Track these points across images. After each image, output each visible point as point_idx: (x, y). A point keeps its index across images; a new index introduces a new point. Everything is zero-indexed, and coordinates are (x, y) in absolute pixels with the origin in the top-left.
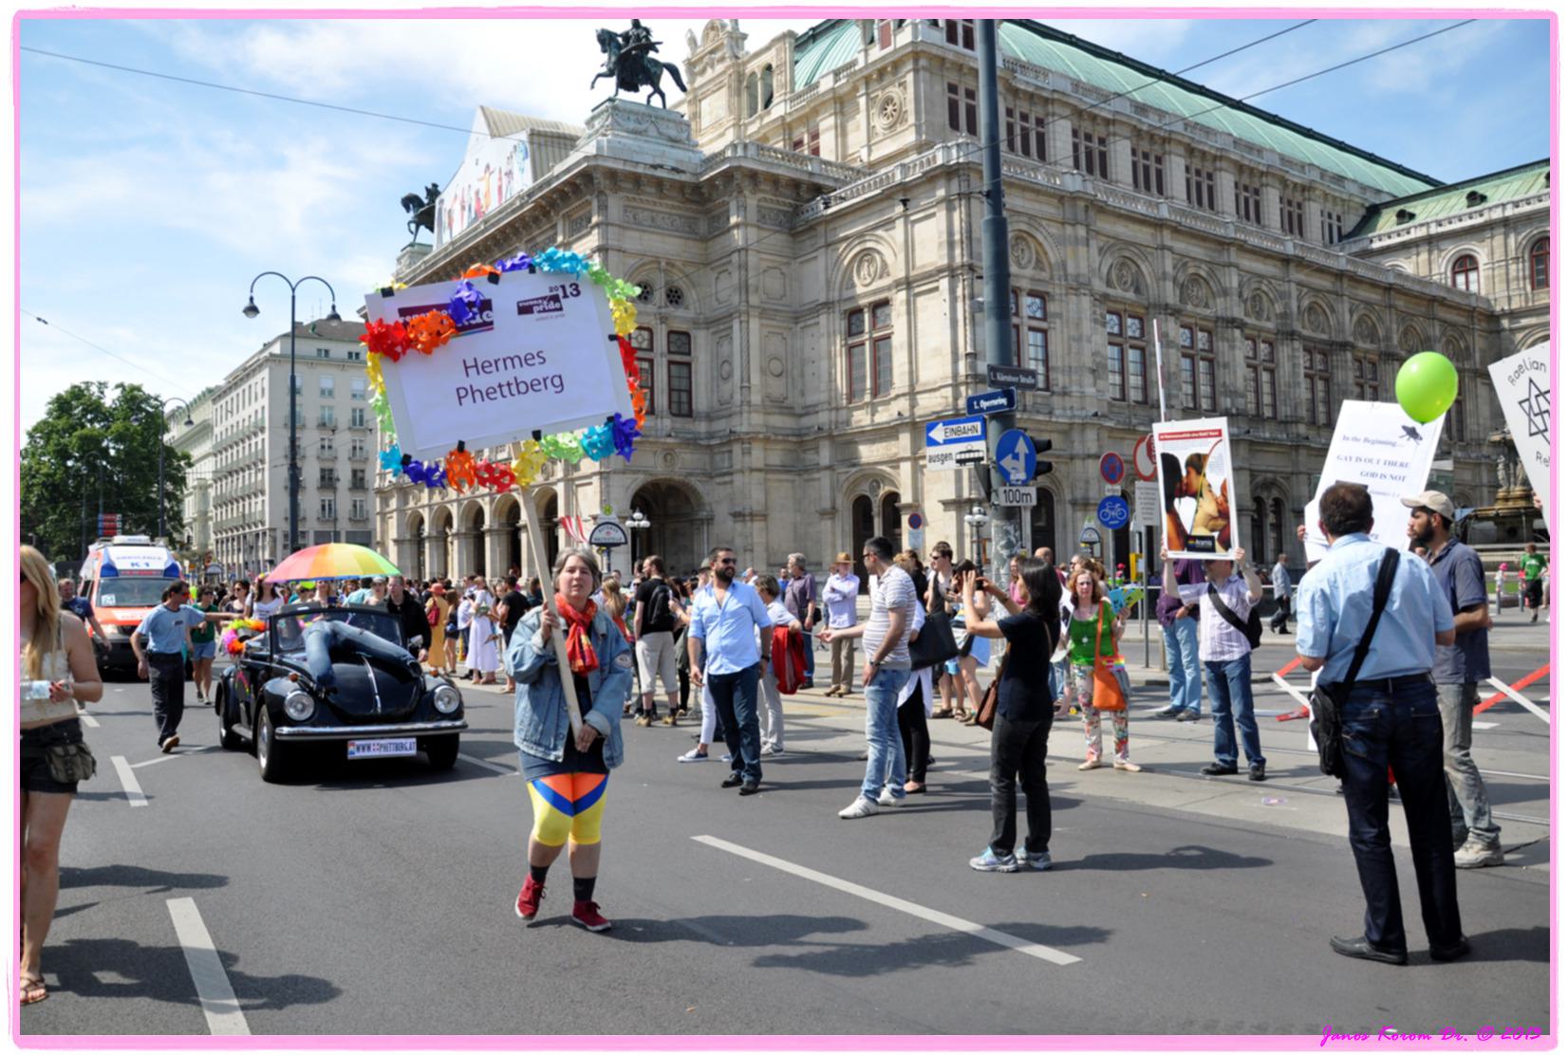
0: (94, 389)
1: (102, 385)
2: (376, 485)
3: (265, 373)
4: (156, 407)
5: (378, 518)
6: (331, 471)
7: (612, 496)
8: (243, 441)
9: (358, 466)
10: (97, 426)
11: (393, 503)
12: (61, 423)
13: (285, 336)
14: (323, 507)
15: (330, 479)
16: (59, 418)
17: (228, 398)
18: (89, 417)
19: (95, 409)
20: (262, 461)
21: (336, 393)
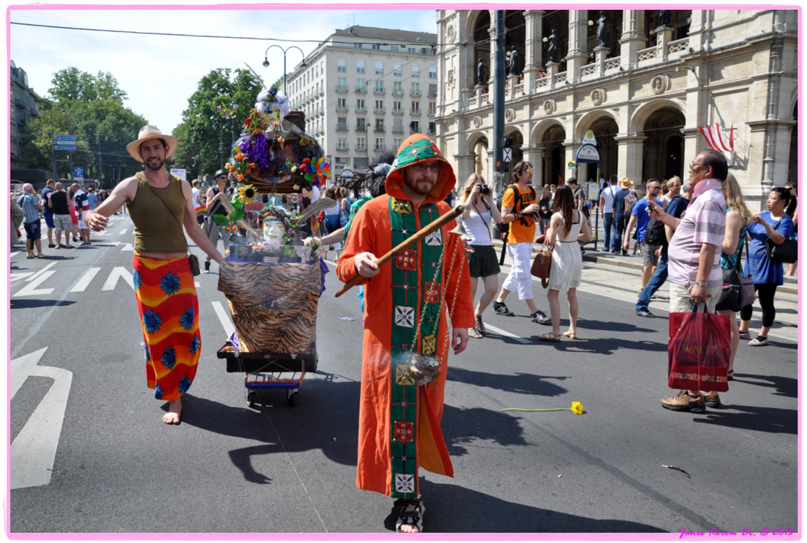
0: (223, 73)
1: (228, 71)
2: (437, 114)
3: (324, 59)
4: (258, 83)
5: (438, 140)
6: (363, 120)
7: (781, 101)
8: (308, 103)
9: (380, 117)
10: (226, 94)
11: (454, 128)
12: (206, 93)
13: (335, 35)
14: (359, 145)
15: (363, 125)
16: (205, 91)
17: (298, 79)
18: (221, 90)
19: (224, 85)
20: (322, 114)
21: (366, 71)
